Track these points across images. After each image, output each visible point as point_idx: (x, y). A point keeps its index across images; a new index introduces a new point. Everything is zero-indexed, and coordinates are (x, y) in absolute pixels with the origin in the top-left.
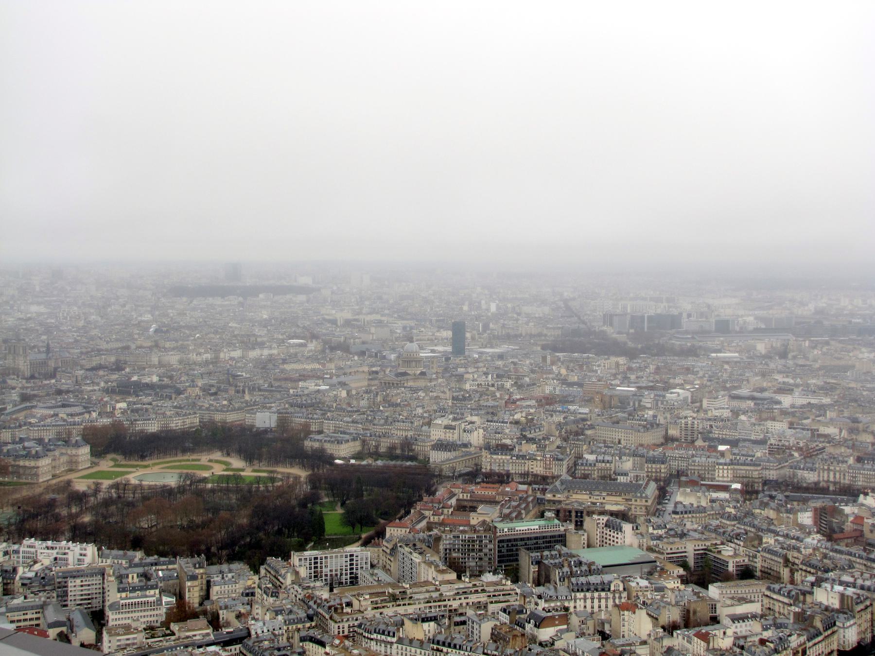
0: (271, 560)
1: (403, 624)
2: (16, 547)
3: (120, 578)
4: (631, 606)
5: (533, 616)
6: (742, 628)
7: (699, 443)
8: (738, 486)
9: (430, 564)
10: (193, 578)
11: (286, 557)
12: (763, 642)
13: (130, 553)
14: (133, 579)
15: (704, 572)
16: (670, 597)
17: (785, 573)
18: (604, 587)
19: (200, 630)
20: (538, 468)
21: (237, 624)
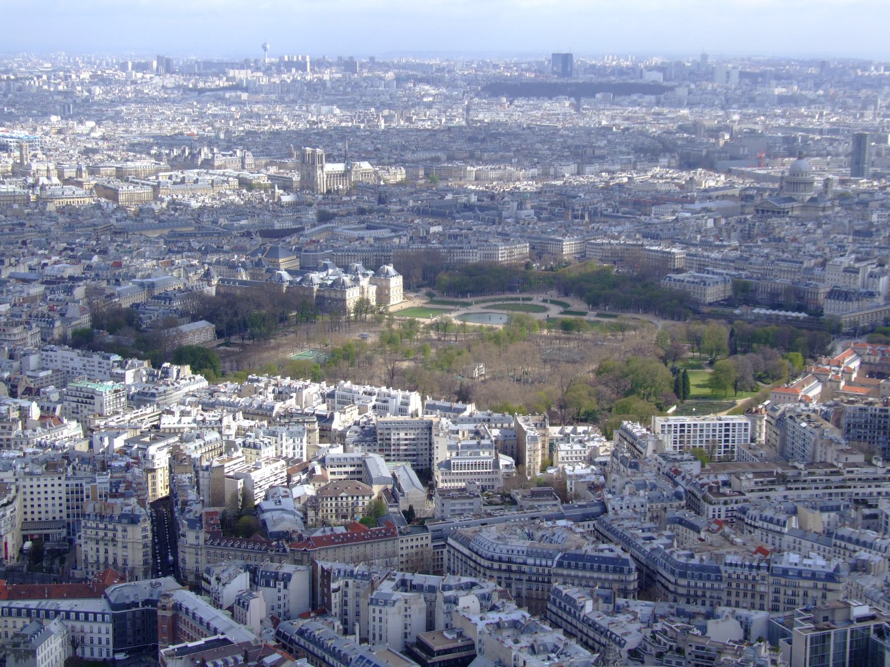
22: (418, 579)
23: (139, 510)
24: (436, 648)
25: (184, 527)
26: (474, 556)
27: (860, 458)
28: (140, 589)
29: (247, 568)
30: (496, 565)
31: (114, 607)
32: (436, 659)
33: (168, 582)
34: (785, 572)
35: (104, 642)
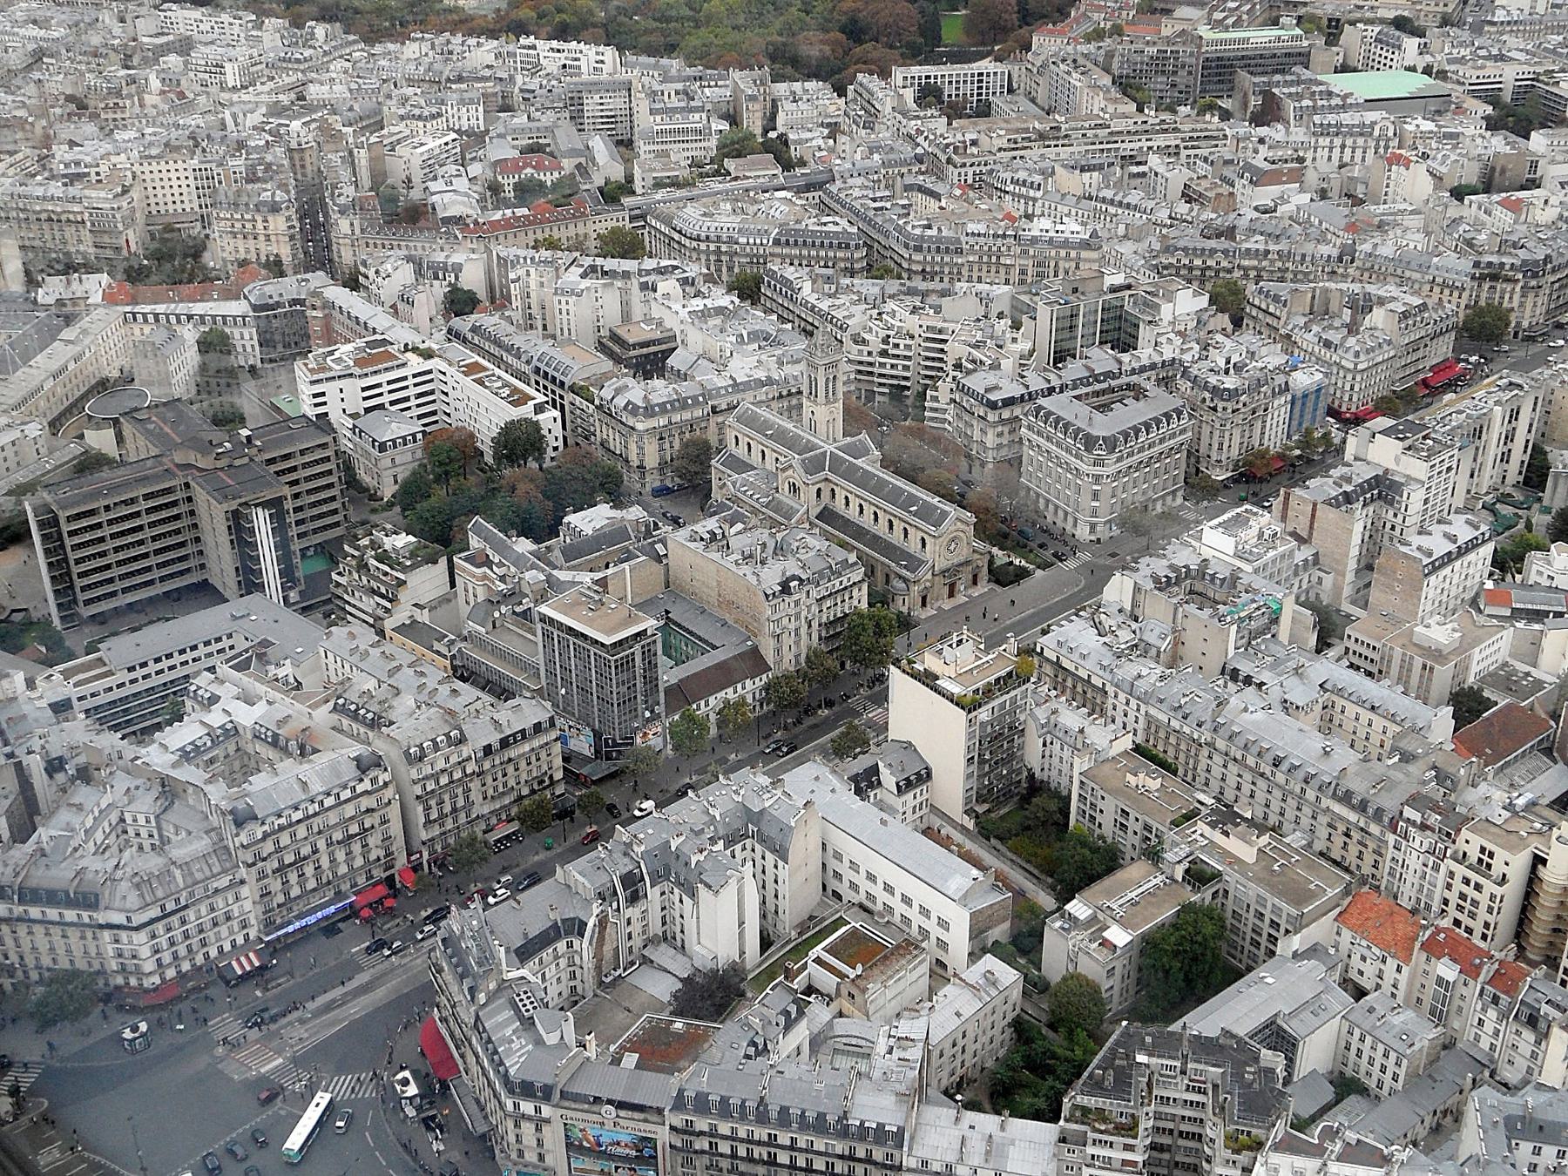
2: (511, 48)
3: (653, 95)
5: (1248, 167)
11: (885, 74)
13: (664, 61)
19: (764, 170)
22: (610, 264)
23: (280, 196)
24: (631, 341)
26: (676, 236)
28: (288, 287)
29: (409, 259)
30: (703, 246)
31: (255, 308)
32: (632, 353)
33: (318, 278)
34: (1034, 241)
35: (249, 349)
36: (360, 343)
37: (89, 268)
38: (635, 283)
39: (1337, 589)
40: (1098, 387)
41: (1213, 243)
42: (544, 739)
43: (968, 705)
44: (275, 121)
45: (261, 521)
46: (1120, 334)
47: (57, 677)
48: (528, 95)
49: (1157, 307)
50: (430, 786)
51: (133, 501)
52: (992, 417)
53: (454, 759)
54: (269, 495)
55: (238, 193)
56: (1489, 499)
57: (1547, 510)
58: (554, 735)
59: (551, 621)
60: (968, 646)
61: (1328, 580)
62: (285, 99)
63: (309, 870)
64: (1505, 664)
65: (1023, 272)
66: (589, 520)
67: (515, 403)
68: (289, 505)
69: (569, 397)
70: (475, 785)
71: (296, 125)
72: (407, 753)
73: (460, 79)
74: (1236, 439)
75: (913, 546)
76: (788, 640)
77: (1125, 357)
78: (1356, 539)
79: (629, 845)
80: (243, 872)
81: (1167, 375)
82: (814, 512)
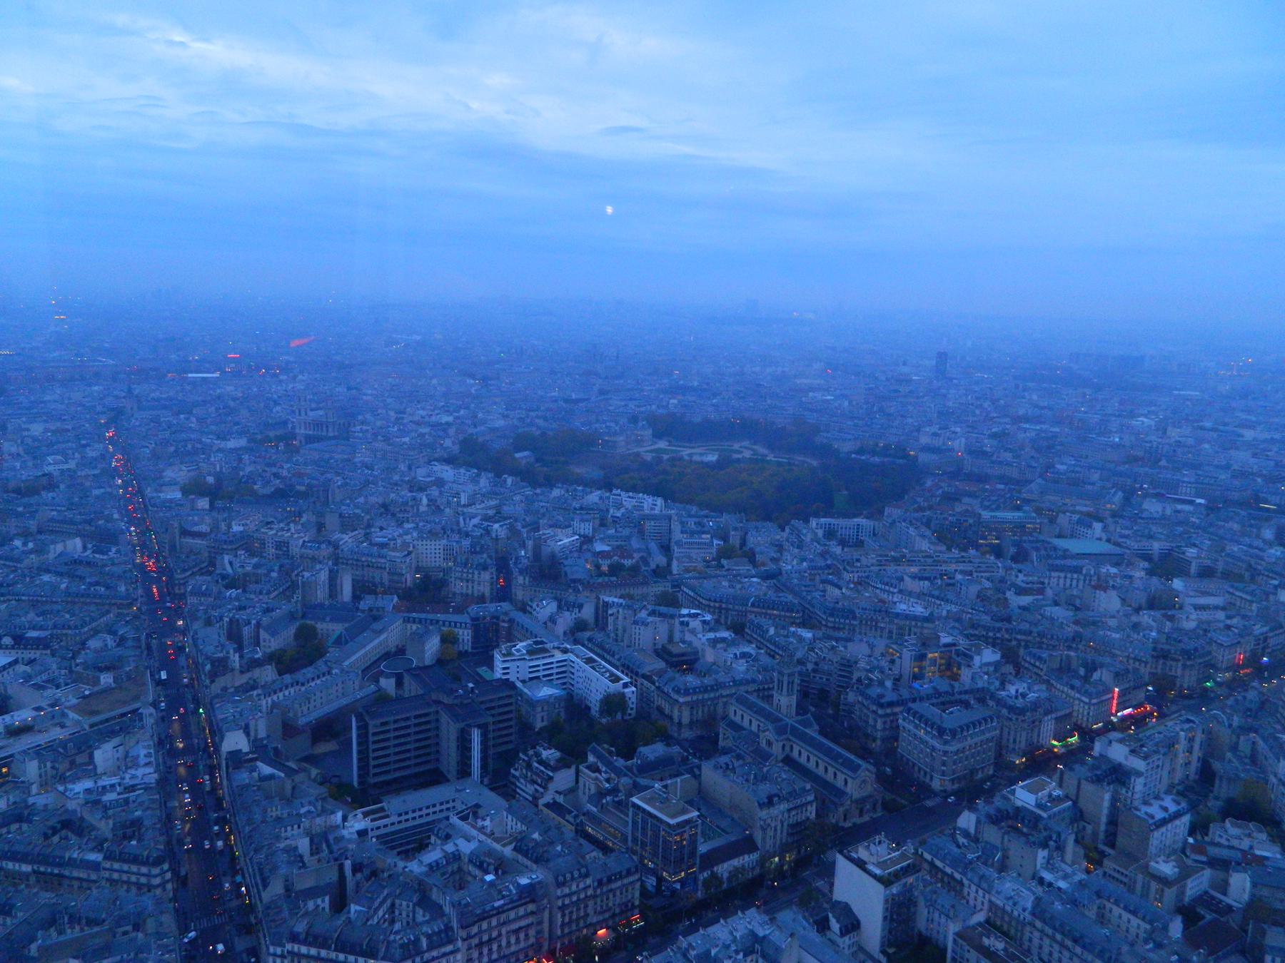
0: (795, 522)
1: (902, 579)
3: (682, 523)
4: (1102, 585)
5: (1014, 585)
6: (1205, 615)
7: (1163, 463)
8: (1202, 501)
9: (923, 536)
10: (735, 529)
11: (807, 521)
12: (1228, 627)
14: (691, 524)
15: (1167, 566)
16: (1138, 584)
17: (1247, 575)
18: (1077, 570)
19: (745, 568)
20: (1013, 473)
21: (771, 567)
22: (663, 609)
25: (515, 572)
27: (944, 548)
29: (555, 598)
33: (506, 606)
34: (897, 615)
36: (529, 642)
37: (389, 591)
38: (677, 621)
39: (1095, 834)
40: (941, 699)
41: (998, 625)
42: (631, 879)
43: (886, 882)
44: (486, 524)
45: (476, 736)
46: (949, 668)
47: (360, 816)
48: (616, 520)
49: (971, 658)
50: (567, 902)
51: (408, 719)
52: (880, 712)
53: (582, 886)
54: (482, 721)
55: (467, 559)
56: (1180, 788)
57: (1217, 798)
58: (636, 877)
59: (639, 807)
60: (884, 846)
61: (1089, 828)
62: (491, 512)
63: (495, 947)
64: (1206, 893)
65: (890, 632)
66: (653, 751)
67: (613, 681)
68: (491, 728)
69: (640, 680)
70: (591, 903)
71: (496, 526)
72: (556, 878)
73: (581, 508)
74: (1023, 739)
75: (839, 783)
76: (770, 833)
77: (956, 684)
78: (1106, 804)
79: (687, 950)
80: (460, 943)
81: (982, 696)
82: (780, 758)
